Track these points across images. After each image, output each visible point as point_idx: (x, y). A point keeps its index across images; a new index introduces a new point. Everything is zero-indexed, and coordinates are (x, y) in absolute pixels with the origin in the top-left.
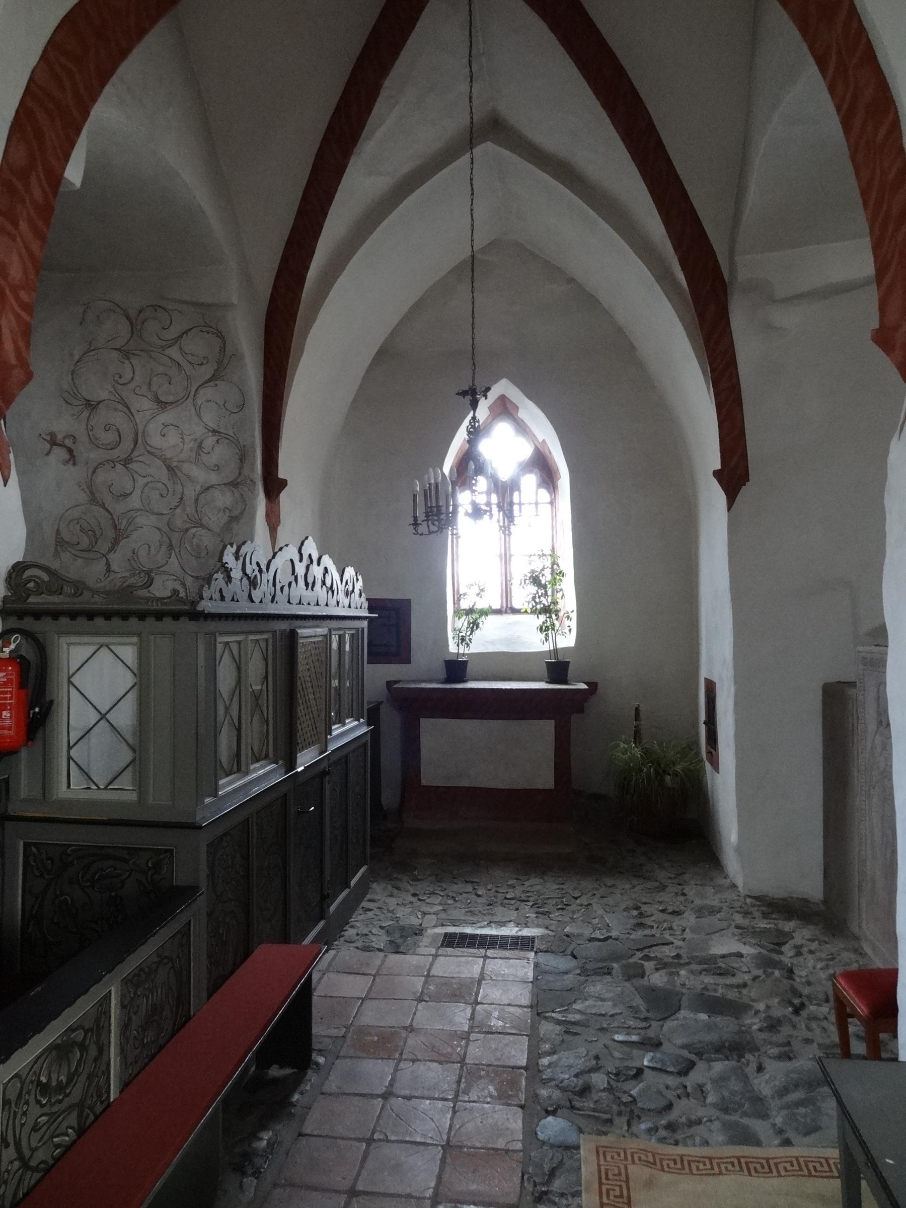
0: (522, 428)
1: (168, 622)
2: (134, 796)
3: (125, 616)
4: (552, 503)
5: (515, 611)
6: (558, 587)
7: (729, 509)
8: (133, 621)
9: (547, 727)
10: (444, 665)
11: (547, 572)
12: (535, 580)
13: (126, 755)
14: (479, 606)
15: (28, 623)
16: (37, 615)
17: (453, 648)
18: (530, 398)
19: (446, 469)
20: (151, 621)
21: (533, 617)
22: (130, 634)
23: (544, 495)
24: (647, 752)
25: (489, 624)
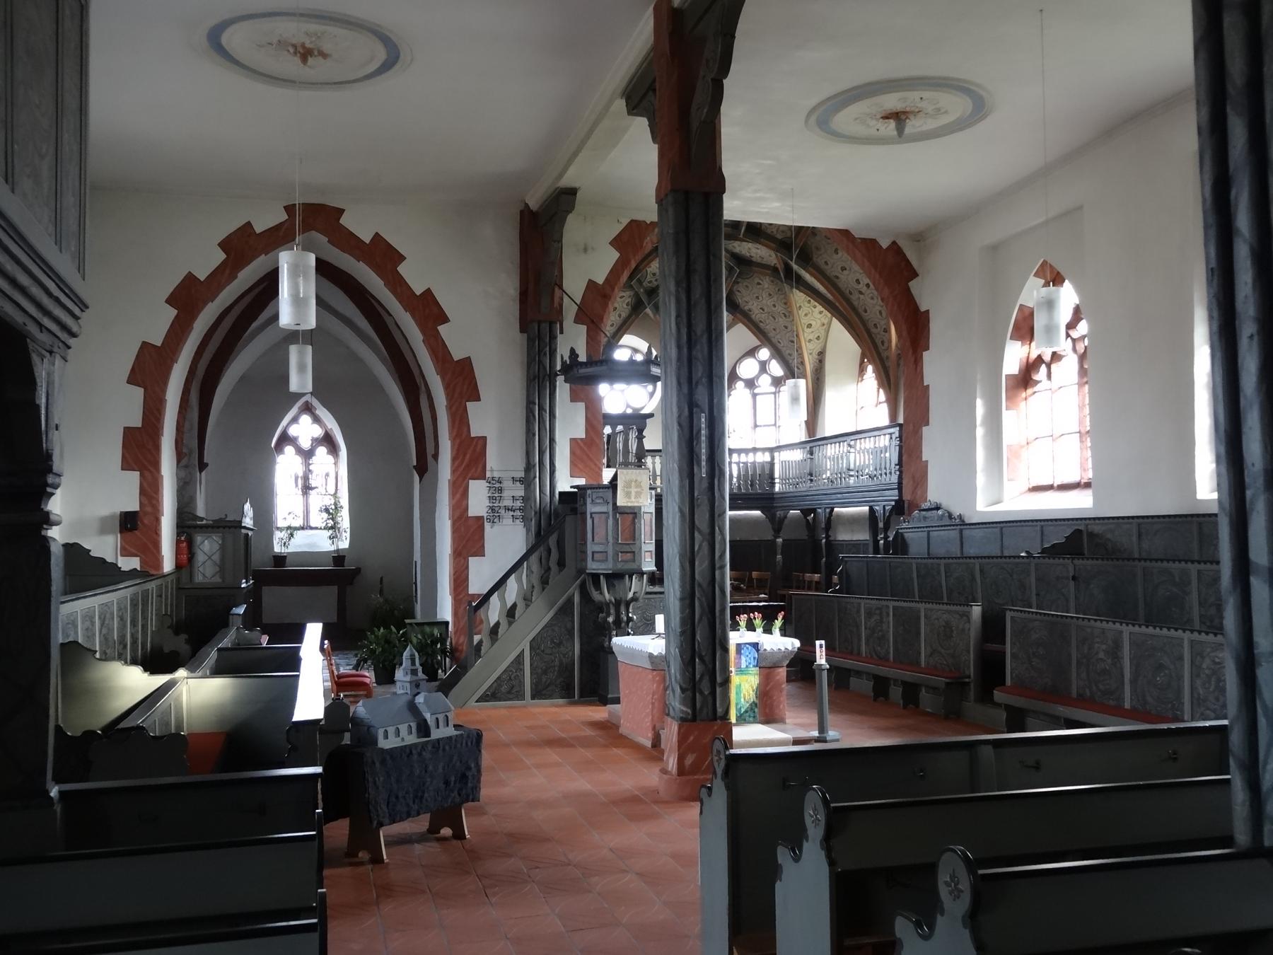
0: (316, 420)
1: (232, 529)
2: (220, 580)
3: (218, 527)
4: (336, 464)
5: (312, 528)
6: (339, 515)
7: (420, 482)
8: (221, 529)
9: (334, 589)
10: (272, 558)
11: (333, 507)
12: (327, 510)
13: (218, 569)
14: (293, 525)
15: (186, 529)
16: (189, 527)
17: (277, 549)
18: (325, 407)
19: (273, 445)
20: (227, 529)
21: (326, 531)
22: (218, 532)
23: (331, 459)
24: (386, 601)
25: (299, 535)
